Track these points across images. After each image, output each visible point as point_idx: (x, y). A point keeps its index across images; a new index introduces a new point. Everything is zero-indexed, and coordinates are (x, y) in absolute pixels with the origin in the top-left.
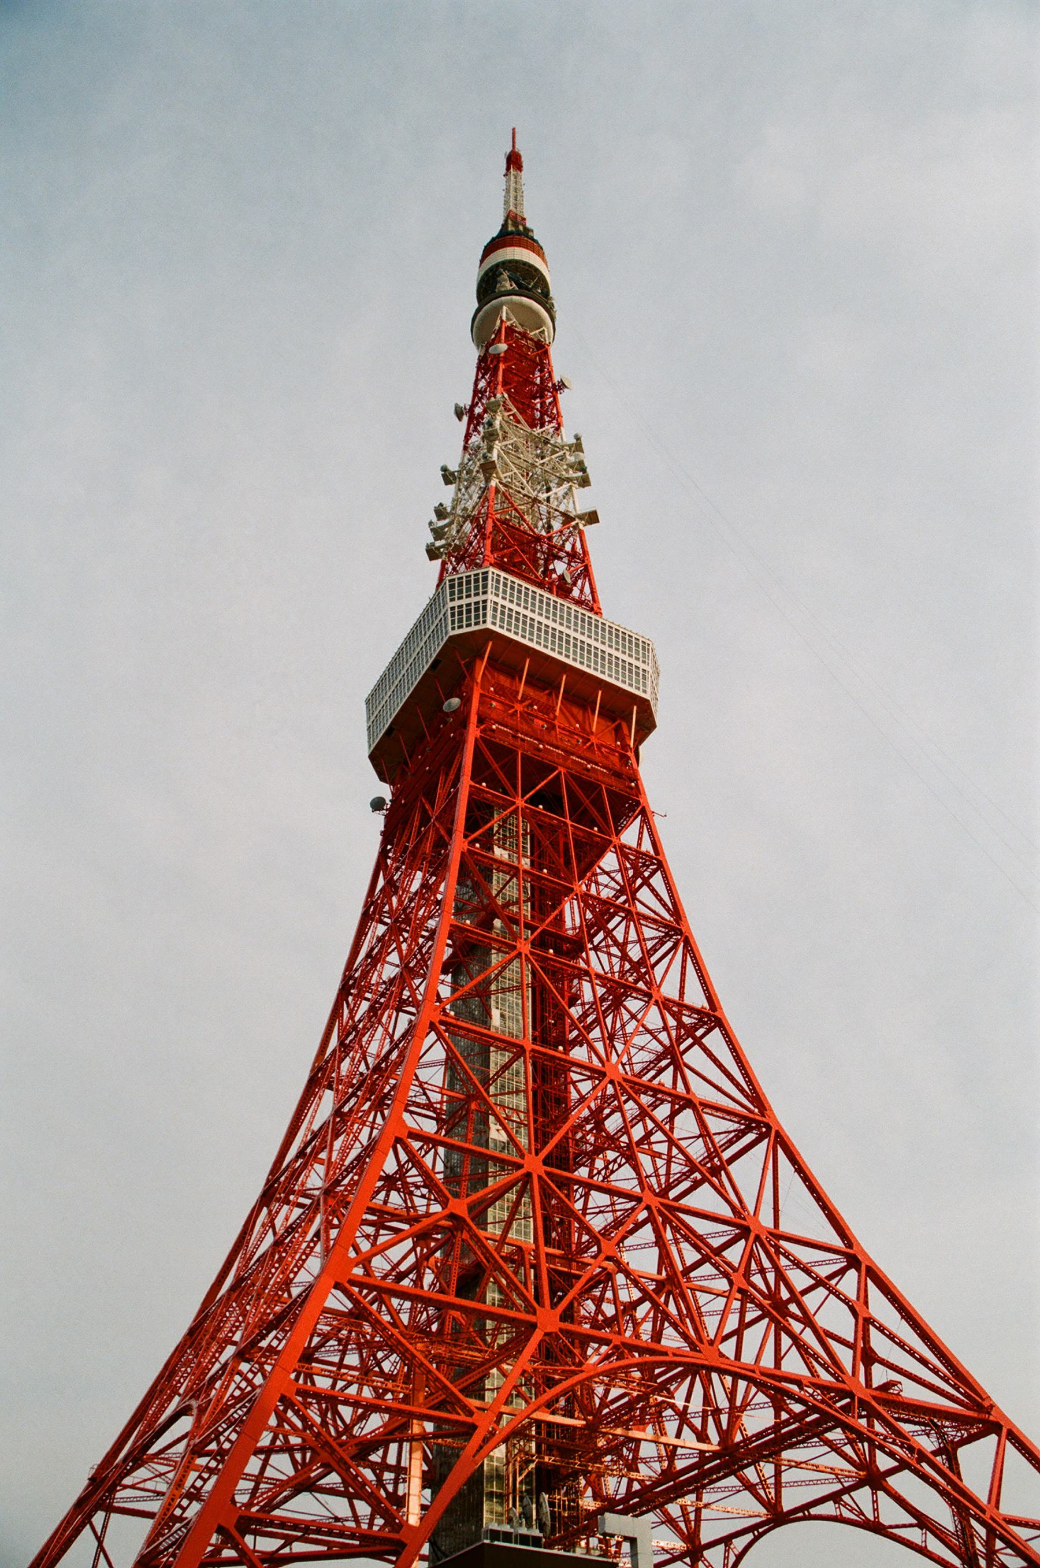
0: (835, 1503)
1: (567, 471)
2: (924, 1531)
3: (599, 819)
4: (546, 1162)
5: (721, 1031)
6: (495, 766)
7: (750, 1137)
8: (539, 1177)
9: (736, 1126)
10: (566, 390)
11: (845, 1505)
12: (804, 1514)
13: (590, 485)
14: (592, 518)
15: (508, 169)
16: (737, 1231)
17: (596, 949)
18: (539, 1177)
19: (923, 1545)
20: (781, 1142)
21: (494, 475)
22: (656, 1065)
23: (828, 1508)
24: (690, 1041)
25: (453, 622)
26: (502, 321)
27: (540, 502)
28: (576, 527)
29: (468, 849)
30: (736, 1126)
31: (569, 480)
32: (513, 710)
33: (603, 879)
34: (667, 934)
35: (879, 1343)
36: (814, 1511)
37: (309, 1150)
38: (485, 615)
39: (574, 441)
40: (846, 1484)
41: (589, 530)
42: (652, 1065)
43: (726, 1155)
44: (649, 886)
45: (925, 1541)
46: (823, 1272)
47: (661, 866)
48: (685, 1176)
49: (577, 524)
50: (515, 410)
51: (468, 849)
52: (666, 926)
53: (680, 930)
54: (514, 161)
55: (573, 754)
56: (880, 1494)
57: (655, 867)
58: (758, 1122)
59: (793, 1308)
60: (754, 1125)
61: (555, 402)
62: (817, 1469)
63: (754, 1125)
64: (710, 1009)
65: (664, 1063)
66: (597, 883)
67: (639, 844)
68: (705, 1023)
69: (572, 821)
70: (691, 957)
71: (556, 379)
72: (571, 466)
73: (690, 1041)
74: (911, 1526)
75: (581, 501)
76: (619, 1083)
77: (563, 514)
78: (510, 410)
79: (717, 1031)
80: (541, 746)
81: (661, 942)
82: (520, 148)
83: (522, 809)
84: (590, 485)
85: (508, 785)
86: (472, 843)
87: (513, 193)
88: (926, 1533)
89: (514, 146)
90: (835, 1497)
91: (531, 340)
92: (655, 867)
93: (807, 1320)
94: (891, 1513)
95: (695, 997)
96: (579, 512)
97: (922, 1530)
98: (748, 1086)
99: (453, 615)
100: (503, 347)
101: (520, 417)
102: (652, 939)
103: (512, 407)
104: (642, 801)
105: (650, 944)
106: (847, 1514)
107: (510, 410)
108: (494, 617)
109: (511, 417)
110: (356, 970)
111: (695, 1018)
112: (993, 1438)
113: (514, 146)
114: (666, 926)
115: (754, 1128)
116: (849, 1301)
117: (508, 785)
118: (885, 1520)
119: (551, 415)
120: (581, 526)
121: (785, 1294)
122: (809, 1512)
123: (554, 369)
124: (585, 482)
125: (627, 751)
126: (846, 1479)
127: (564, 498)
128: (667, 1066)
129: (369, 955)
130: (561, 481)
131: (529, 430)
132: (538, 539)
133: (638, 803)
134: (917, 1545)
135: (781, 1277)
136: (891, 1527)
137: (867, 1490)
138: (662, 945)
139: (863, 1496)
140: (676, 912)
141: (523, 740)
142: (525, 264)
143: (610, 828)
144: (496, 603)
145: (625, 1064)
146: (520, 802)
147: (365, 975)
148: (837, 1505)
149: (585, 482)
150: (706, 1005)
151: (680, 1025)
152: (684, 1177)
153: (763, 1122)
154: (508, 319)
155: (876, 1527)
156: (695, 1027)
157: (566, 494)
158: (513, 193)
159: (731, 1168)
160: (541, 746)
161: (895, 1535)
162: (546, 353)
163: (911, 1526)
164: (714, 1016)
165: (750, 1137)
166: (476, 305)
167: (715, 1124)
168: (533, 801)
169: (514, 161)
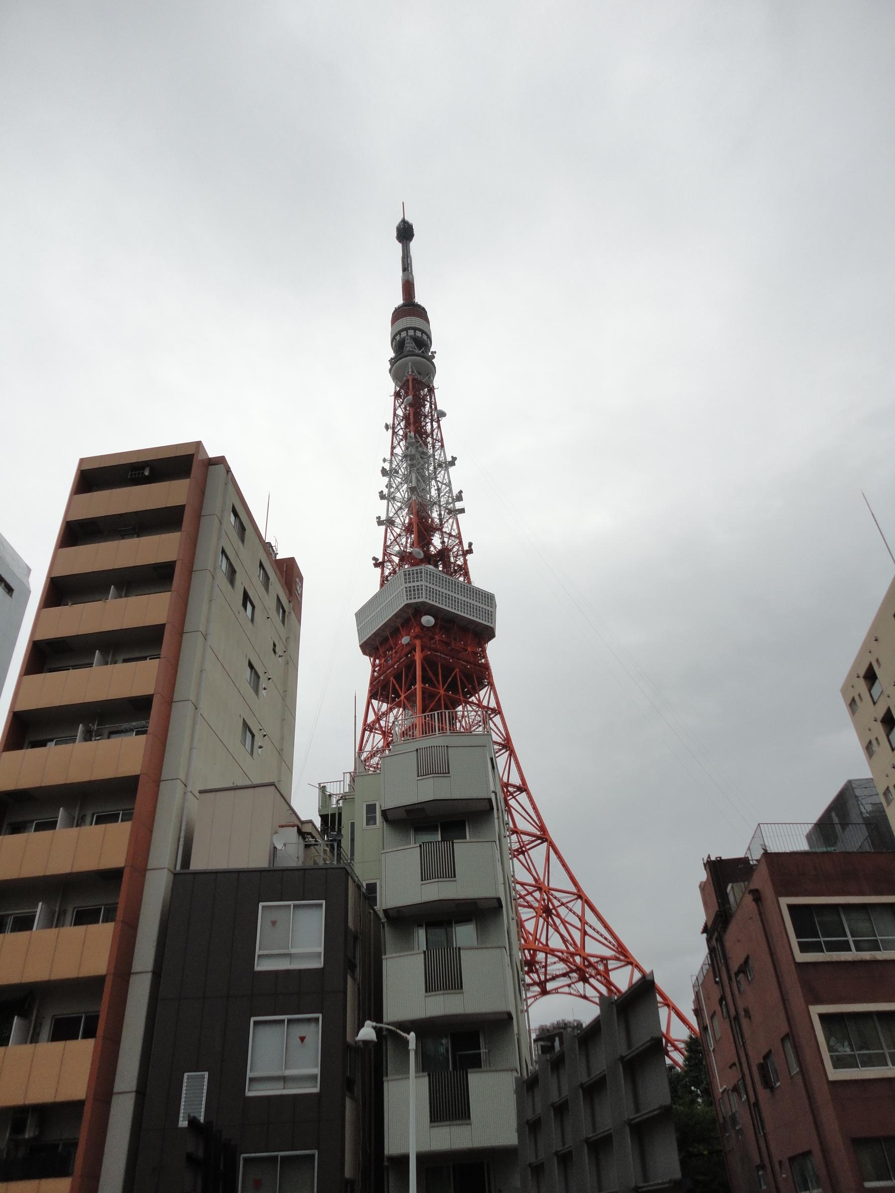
11: (572, 988)
20: (551, 845)
24: (511, 797)
25: (407, 595)
36: (559, 990)
38: (422, 593)
39: (449, 459)
43: (528, 847)
59: (554, 911)
93: (558, 916)
95: (515, 780)
99: (406, 591)
108: (426, 594)
112: (630, 967)
121: (551, 907)
135: (549, 900)
144: (427, 586)
159: (529, 852)
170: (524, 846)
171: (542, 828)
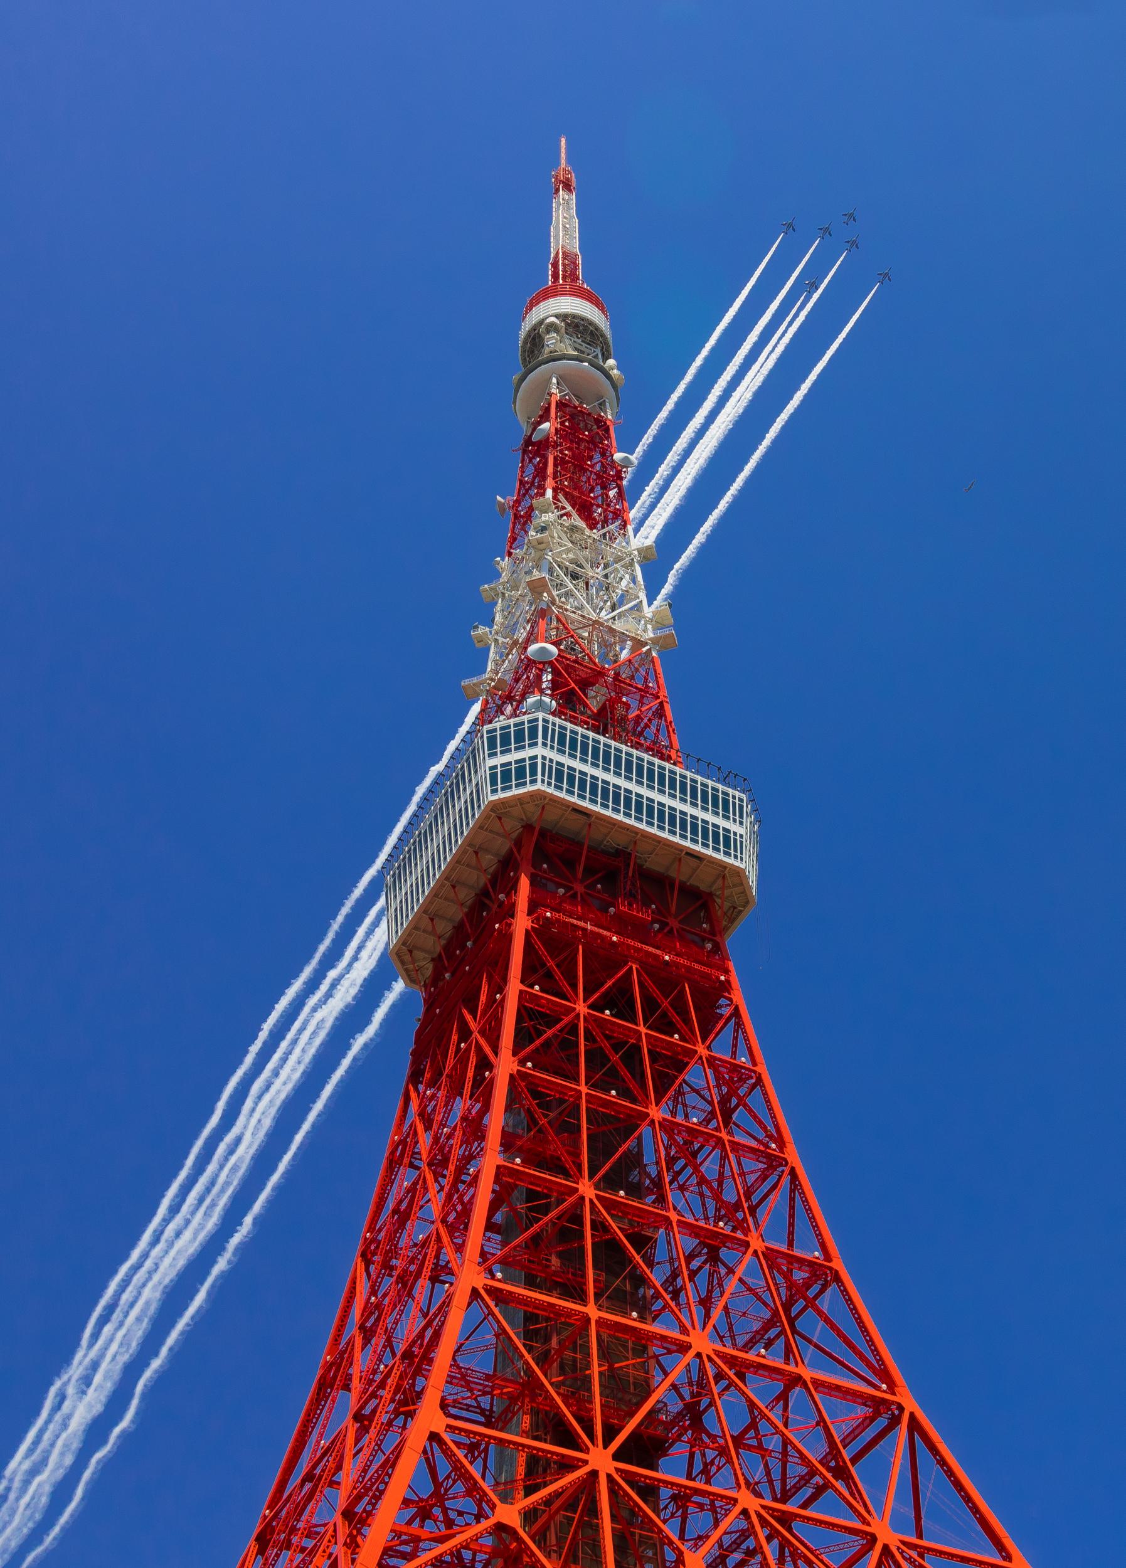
4: (616, 1457)
5: (839, 1287)
7: (882, 1422)
8: (609, 1476)
16: (861, 1542)
17: (682, 1188)
18: (609, 1476)
22: (763, 1335)
29: (518, 1070)
33: (691, 1099)
37: (318, 1471)
42: (758, 1337)
44: (745, 1105)
48: (805, 1480)
51: (518, 1070)
53: (785, 1160)
64: (825, 1260)
65: (772, 1333)
66: (685, 1105)
69: (648, 1028)
70: (800, 1194)
73: (801, 1303)
76: (709, 1357)
79: (833, 1287)
81: (764, 1178)
85: (566, 987)
86: (522, 1062)
92: (753, 1081)
98: (878, 1361)
102: (752, 1172)
105: (751, 1179)
110: (380, 1230)
117: (566, 987)
128: (778, 1336)
129: (396, 1211)
138: (764, 1180)
145: (724, 1337)
146: (582, 1008)
147: (392, 1237)
151: (791, 1285)
152: (803, 1482)
156: (807, 1285)
165: (882, 1422)
168: (597, 1007)
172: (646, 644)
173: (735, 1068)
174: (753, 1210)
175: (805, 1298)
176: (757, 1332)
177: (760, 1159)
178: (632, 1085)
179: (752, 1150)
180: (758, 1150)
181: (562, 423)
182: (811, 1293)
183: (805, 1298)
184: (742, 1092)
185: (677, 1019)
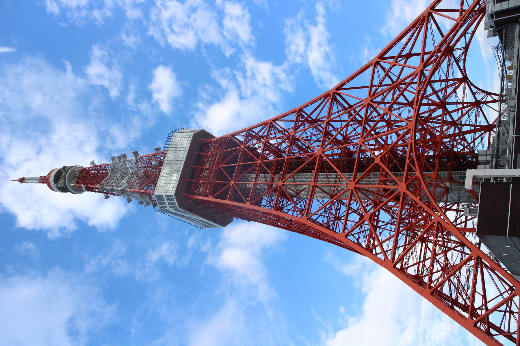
0: (459, 62)
1: (121, 162)
2: (467, 33)
3: (236, 153)
6: (221, 191)
7: (338, 97)
9: (335, 103)
10: (95, 162)
12: (463, 71)
13: (125, 154)
14: (136, 154)
15: (25, 182)
19: (471, 33)
21: (125, 189)
23: (461, 64)
26: (75, 185)
27: (132, 172)
28: (139, 159)
30: (335, 103)
31: (124, 161)
32: (202, 184)
34: (272, 127)
35: (404, 53)
40: (453, 60)
41: (141, 154)
45: (470, 32)
46: (382, 74)
47: (250, 129)
49: (138, 158)
50: (103, 181)
52: (270, 128)
53: (270, 123)
54: (22, 180)
55: (215, 162)
56: (455, 48)
57: (250, 131)
58: (333, 95)
60: (334, 97)
61: (100, 166)
62: (448, 71)
63: (334, 97)
67: (243, 136)
68: (301, 114)
70: (280, 118)
71: (91, 166)
72: (119, 161)
74: (465, 37)
75: (131, 157)
77: (136, 164)
78: (103, 183)
80: (213, 174)
82: (18, 178)
83: (234, 182)
84: (125, 154)
87: (33, 180)
88: (467, 32)
89: (17, 180)
90: (457, 62)
91: (79, 175)
92: (250, 131)
94: (461, 44)
96: (134, 158)
97: (466, 34)
98: (322, 99)
100: (82, 185)
101: (105, 179)
103: (102, 182)
104: (229, 136)
106: (463, 58)
107: (103, 183)
109: (105, 183)
111: (300, 117)
113: (17, 180)
114: (270, 128)
115: (335, 97)
116: (391, 67)
118: (464, 46)
119: (103, 167)
120: (139, 157)
122: (463, 69)
123: (88, 167)
124: (124, 156)
125: (212, 141)
126: (451, 60)
127: (131, 162)
130: (125, 164)
131: (109, 177)
132: (145, 173)
133: (229, 137)
134: (471, 35)
136: (466, 43)
137: (454, 52)
139: (457, 54)
140: (265, 124)
141: (212, 180)
142: (55, 178)
143: (238, 149)
148: (460, 61)
149: (124, 156)
150: (295, 113)
153: (333, 94)
154: (74, 183)
155: (466, 48)
157: (129, 162)
158: (33, 180)
160: (213, 174)
161: (469, 42)
162: (84, 169)
163: (465, 37)
164: (298, 111)
165: (338, 97)
166: (69, 193)
167: (335, 110)
169: (22, 180)
170: (345, 109)
171: (326, 96)
172: (137, 160)
173: (247, 136)
174: (285, 130)
175: (308, 118)
176: (316, 129)
177: (271, 130)
178: (252, 168)
179: (268, 132)
180: (268, 130)
181: (82, 183)
182: (306, 116)
183: (308, 118)
184: (254, 134)
185: (234, 154)
